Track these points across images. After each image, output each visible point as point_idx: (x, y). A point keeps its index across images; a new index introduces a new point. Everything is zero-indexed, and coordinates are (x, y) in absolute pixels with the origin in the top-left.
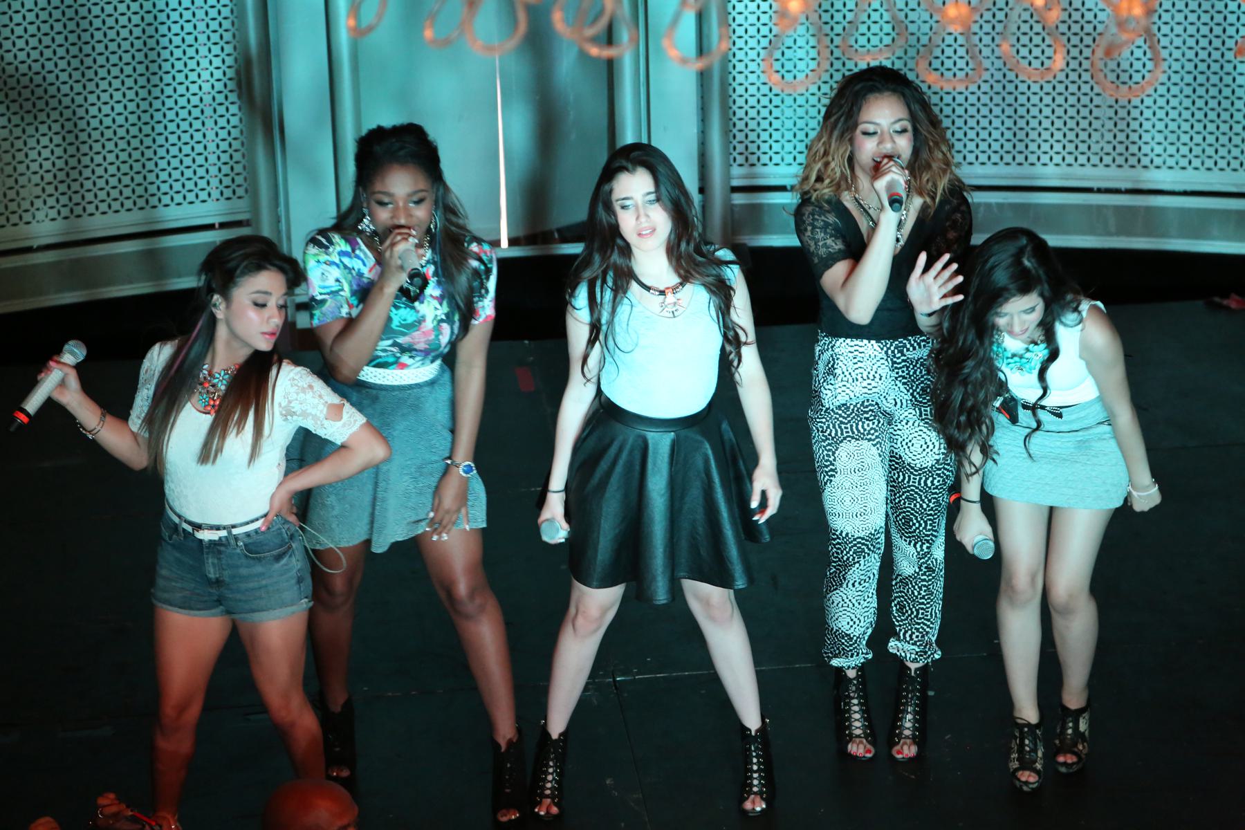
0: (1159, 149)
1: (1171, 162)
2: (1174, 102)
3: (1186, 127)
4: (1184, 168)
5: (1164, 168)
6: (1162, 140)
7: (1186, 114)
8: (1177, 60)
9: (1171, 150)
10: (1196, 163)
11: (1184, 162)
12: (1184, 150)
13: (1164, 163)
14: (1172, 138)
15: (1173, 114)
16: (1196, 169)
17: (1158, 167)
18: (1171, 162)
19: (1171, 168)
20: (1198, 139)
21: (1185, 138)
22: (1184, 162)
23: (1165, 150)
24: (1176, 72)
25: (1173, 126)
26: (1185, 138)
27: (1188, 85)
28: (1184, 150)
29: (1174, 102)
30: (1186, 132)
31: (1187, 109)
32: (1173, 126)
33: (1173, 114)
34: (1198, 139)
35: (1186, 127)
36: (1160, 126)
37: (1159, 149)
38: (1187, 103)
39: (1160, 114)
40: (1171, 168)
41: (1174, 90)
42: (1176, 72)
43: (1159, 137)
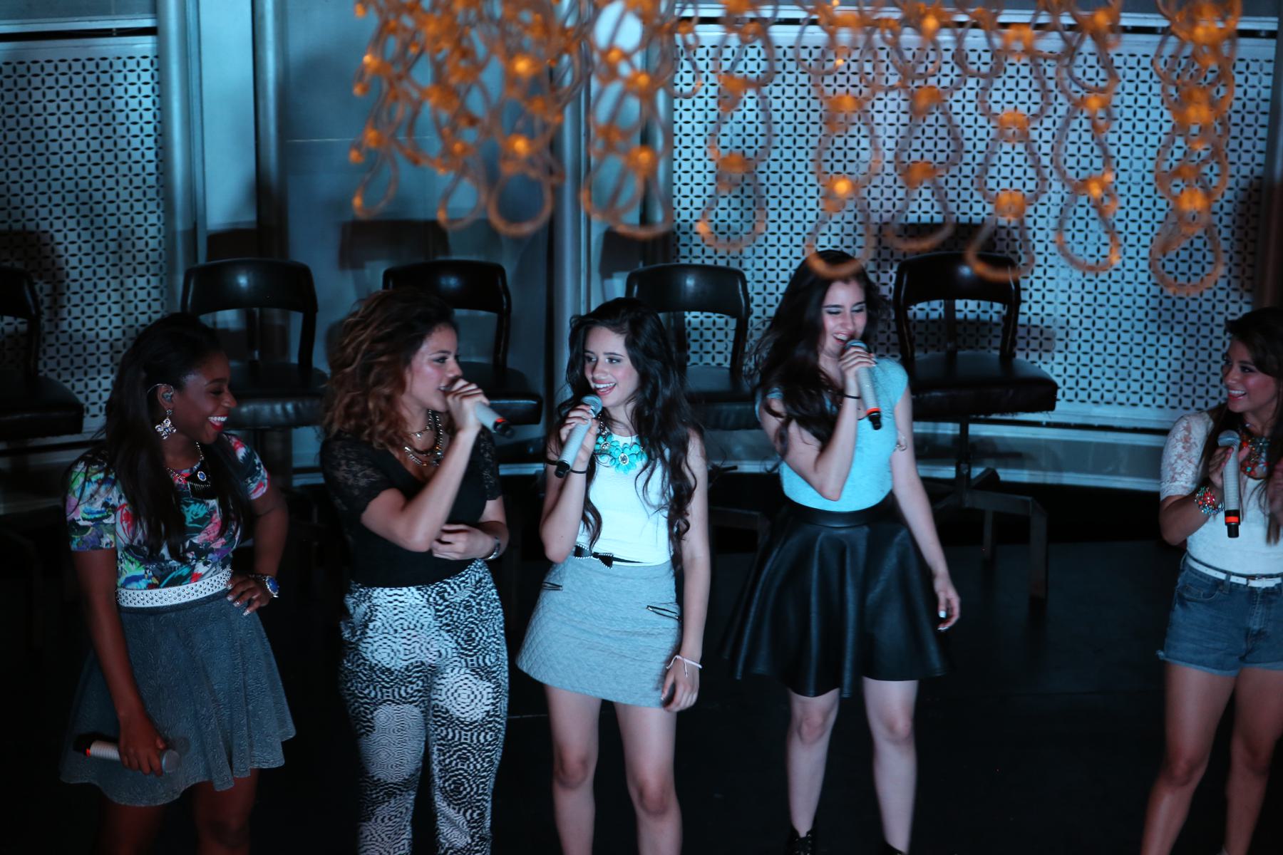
0: (1109, 385)
1: (1121, 398)
2: (1125, 337)
3: (1137, 362)
4: (1134, 405)
5: (1115, 404)
6: (1113, 375)
7: (1138, 350)
8: (1128, 295)
9: (1122, 386)
10: (1147, 400)
11: (1135, 399)
12: (1135, 387)
13: (1115, 399)
14: (1123, 373)
15: (1124, 349)
16: (1147, 406)
17: (1108, 403)
18: (1121, 398)
19: (1121, 404)
20: (1149, 375)
21: (1136, 374)
22: (1135, 399)
23: (1116, 386)
24: (1128, 307)
25: (1123, 361)
26: (1136, 374)
27: (1140, 320)
28: (1135, 387)
29: (1125, 337)
30: (1137, 368)
31: (1138, 344)
32: (1123, 361)
33: (1124, 349)
34: (1149, 375)
35: (1137, 362)
36: (1111, 361)
37: (1109, 385)
38: (1138, 338)
39: (1112, 349)
40: (1121, 404)
41: (1126, 325)
42: (1128, 307)
43: (1110, 373)
